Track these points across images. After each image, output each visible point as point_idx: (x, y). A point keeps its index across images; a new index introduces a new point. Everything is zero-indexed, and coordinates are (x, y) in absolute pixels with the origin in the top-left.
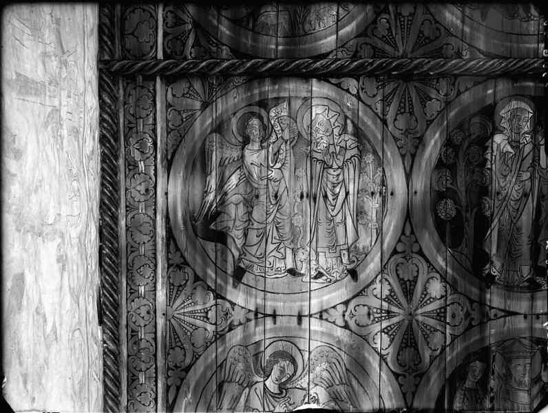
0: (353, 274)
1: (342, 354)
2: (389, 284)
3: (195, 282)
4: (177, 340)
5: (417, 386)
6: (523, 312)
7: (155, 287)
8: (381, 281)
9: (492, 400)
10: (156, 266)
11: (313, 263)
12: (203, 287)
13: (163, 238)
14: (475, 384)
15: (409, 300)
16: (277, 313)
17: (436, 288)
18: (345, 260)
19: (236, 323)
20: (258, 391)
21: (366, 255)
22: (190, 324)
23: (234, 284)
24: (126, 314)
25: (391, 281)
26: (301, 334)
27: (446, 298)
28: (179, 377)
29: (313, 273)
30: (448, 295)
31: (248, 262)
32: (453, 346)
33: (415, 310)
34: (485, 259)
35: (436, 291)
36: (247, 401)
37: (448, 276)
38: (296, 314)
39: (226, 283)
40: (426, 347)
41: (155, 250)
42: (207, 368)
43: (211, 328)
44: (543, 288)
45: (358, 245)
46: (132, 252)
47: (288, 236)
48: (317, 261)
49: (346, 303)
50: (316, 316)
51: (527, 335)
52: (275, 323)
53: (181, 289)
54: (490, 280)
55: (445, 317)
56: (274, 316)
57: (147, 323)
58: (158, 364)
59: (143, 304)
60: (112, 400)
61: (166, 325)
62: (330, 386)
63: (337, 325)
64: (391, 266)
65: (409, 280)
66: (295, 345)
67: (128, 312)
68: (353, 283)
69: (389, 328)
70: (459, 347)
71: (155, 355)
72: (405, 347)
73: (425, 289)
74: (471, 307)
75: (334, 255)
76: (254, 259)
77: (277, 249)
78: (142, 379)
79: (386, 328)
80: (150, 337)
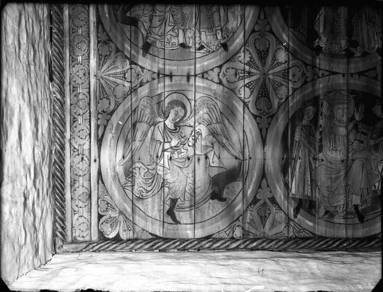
0: (225, 46)
1: (218, 102)
2: (250, 53)
3: (116, 53)
4: (104, 91)
5: (269, 124)
6: (342, 72)
7: (89, 57)
8: (244, 51)
9: (321, 133)
10: (89, 42)
11: (197, 39)
12: (122, 56)
13: (94, 23)
14: (309, 122)
15: (264, 64)
16: (173, 74)
17: (282, 56)
18: (219, 37)
19: (145, 81)
20: (160, 128)
21: (234, 33)
22: (113, 82)
23: (143, 54)
24: (69, 76)
25: (251, 50)
26: (190, 88)
27: (289, 63)
28: (106, 119)
29: (198, 46)
30: (290, 61)
31: (153, 39)
32: (294, 95)
33: (267, 72)
34: (316, 35)
35: (282, 58)
36: (152, 135)
37: (290, 47)
38: (186, 74)
39: (138, 52)
40: (275, 97)
41: (89, 31)
42: (125, 112)
43: (127, 85)
44: (355, 55)
45: (228, 26)
46: (73, 32)
47: (180, 21)
48: (200, 37)
49: (220, 67)
50: (200, 76)
51: (345, 88)
52: (171, 81)
53: (106, 58)
54: (319, 50)
55: (288, 76)
56: (171, 76)
57: (84, 81)
58: (91, 111)
59: (80, 68)
60: (60, 134)
61: (97, 83)
62: (209, 125)
63: (214, 82)
64: (251, 40)
65: (263, 51)
66: (184, 95)
67: (71, 74)
68: (225, 53)
69: (250, 84)
70: (298, 97)
71: (89, 104)
72: (261, 97)
73: (274, 56)
74: (306, 68)
75: (212, 33)
76: (157, 37)
77: (173, 30)
78: (80, 120)
79: (248, 84)
80: (85, 91)
